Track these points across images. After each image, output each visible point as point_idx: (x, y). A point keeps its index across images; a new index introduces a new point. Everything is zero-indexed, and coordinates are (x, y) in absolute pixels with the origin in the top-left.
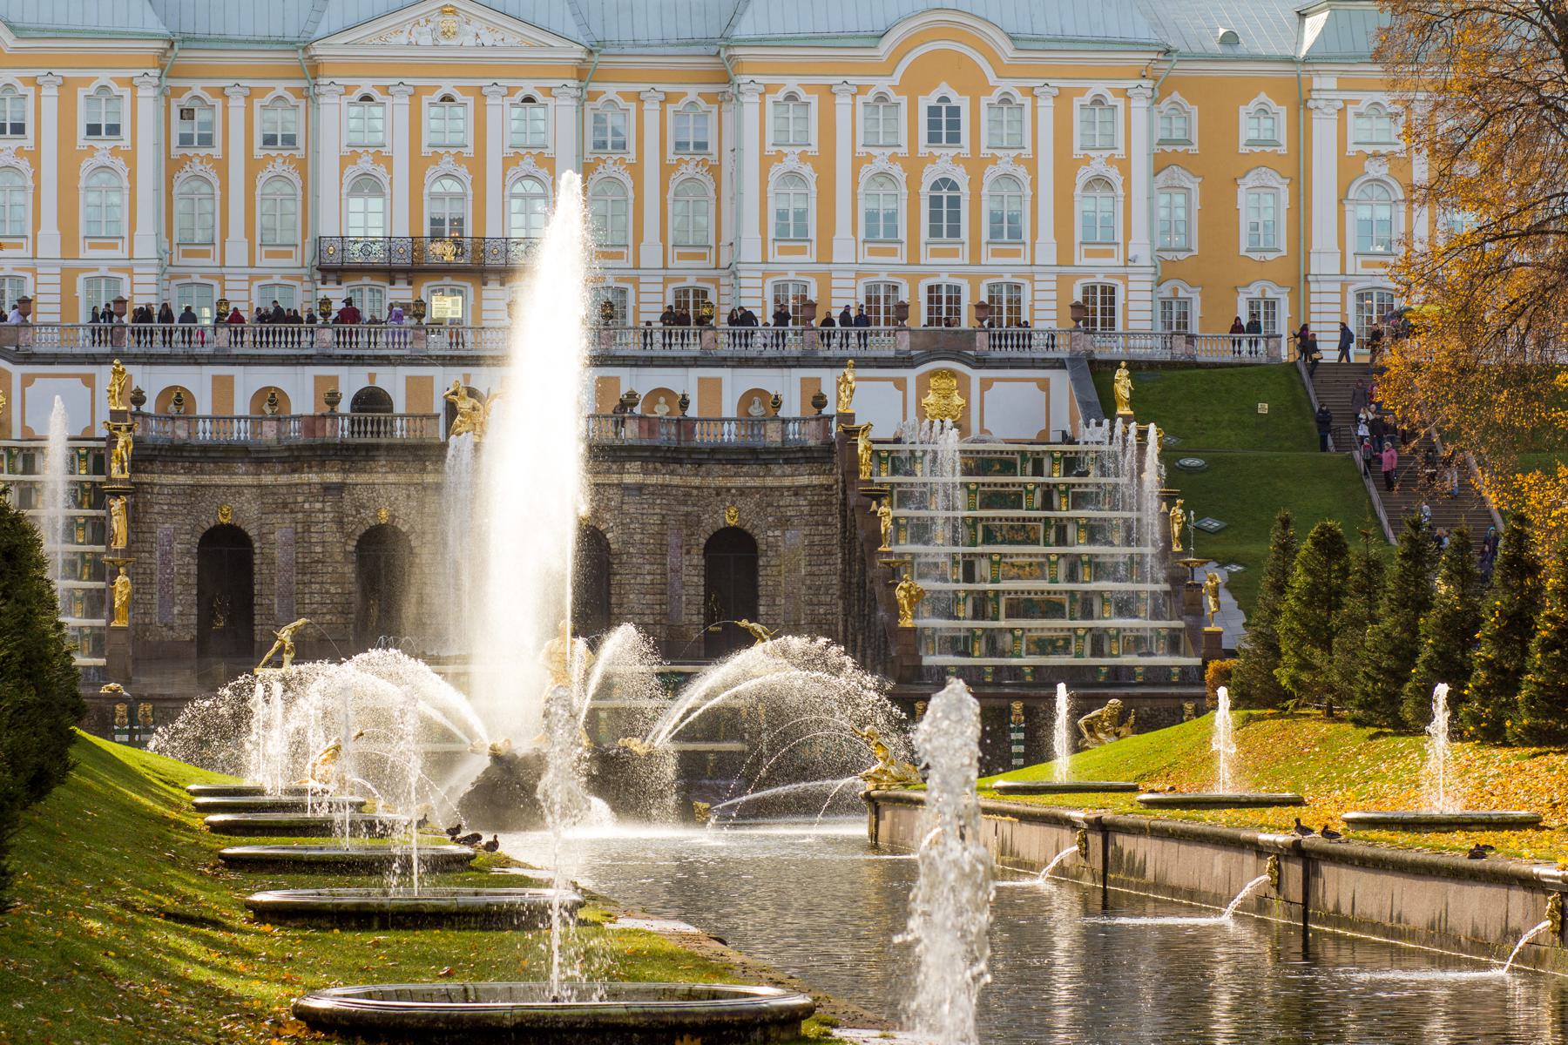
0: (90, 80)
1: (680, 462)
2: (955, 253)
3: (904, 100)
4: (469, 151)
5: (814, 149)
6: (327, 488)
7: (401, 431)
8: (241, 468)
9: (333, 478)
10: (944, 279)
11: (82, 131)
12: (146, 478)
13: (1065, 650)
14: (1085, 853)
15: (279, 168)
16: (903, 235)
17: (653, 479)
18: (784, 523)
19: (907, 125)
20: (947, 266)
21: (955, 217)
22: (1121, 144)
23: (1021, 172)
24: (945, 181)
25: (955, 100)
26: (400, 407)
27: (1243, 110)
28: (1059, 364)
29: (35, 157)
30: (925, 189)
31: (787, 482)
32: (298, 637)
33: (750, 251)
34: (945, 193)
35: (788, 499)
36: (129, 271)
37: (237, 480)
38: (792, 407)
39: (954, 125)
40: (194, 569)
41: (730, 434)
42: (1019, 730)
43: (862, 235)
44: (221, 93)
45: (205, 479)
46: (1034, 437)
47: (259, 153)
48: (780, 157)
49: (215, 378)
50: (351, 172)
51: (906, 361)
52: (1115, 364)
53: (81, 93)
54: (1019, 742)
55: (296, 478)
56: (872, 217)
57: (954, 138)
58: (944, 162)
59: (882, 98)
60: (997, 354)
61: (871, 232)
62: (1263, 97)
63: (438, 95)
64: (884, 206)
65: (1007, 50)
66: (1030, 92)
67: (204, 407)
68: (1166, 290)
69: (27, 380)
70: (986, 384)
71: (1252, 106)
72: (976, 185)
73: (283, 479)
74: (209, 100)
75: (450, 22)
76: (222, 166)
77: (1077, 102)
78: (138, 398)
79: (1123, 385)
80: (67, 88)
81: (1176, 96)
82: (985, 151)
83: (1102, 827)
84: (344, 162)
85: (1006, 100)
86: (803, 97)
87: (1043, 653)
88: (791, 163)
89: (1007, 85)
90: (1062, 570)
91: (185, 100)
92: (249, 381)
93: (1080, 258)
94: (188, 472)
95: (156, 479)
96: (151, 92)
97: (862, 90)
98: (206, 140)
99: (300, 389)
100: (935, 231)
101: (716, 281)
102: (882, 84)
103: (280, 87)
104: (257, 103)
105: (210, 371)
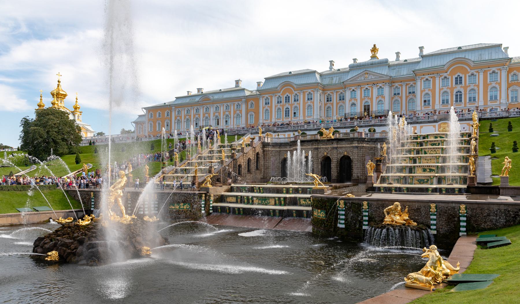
1: (369, 142)
3: (450, 77)
4: (370, 97)
11: (306, 99)
12: (266, 149)
13: (427, 182)
15: (341, 104)
17: (360, 145)
21: (461, 98)
22: (499, 79)
23: (476, 88)
24: (459, 91)
29: (299, 104)
30: (454, 93)
34: (459, 94)
39: (461, 81)
40: (280, 166)
42: (365, 211)
43: (441, 103)
45: (281, 149)
48: (424, 90)
50: (351, 103)
54: (365, 216)
56: (443, 100)
57: (461, 83)
58: (459, 88)
59: (445, 77)
61: (443, 103)
63: (365, 88)
64: (445, 98)
72: (465, 91)
75: (367, 76)
76: (332, 104)
77: (488, 73)
81: (515, 71)
82: (467, 84)
84: (350, 101)
85: (472, 74)
86: (429, 79)
87: (420, 183)
88: (427, 91)
89: (472, 71)
91: (327, 94)
93: (489, 103)
98: (331, 101)
102: (445, 74)
103: (341, 91)
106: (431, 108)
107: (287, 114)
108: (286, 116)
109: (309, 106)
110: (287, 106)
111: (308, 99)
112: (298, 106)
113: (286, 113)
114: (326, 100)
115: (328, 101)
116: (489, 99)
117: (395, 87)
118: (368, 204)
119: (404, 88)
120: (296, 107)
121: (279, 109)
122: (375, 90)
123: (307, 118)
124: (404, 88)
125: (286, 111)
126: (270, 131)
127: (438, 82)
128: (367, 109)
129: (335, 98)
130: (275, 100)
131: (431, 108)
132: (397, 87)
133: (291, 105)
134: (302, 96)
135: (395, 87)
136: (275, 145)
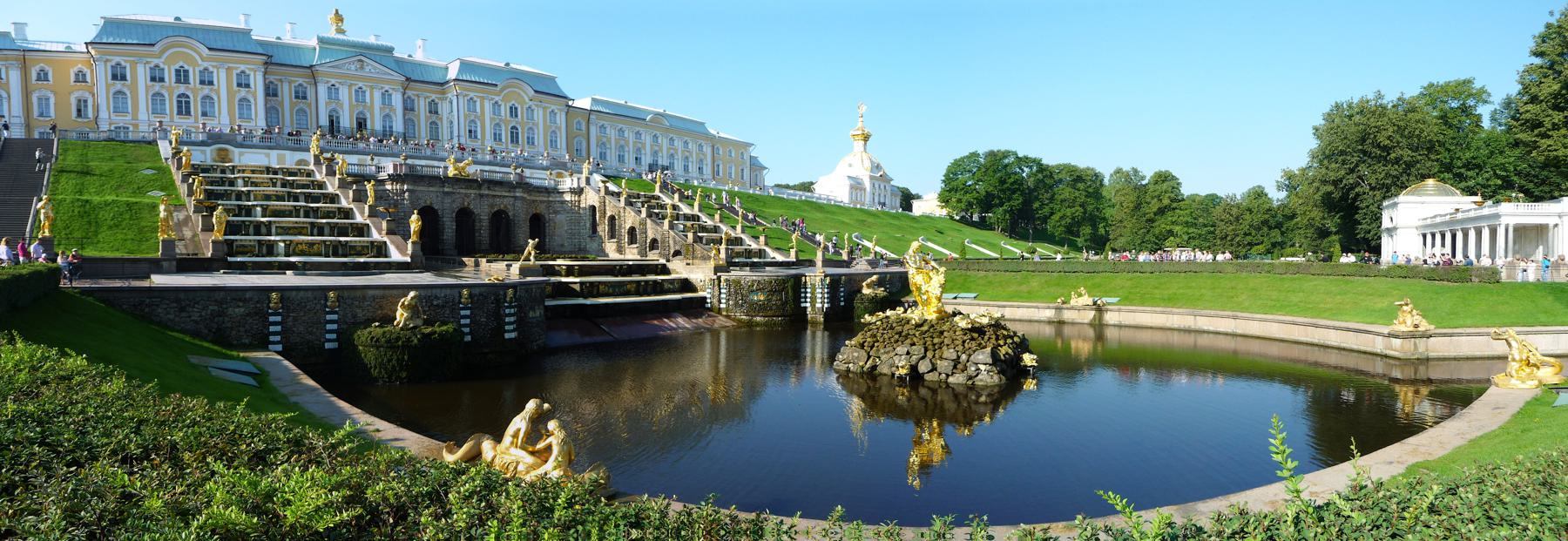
18: (556, 212)
76: (282, 103)
98: (275, 95)
103: (301, 81)
107: (184, 108)
108: (180, 113)
110: (182, 89)
111: (239, 85)
113: (179, 107)
119: (422, 102)
122: (377, 95)
124: (422, 102)
125: (179, 102)
127: (488, 106)
128: (361, 125)
129: (286, 92)
133: (194, 91)
134: (223, 74)
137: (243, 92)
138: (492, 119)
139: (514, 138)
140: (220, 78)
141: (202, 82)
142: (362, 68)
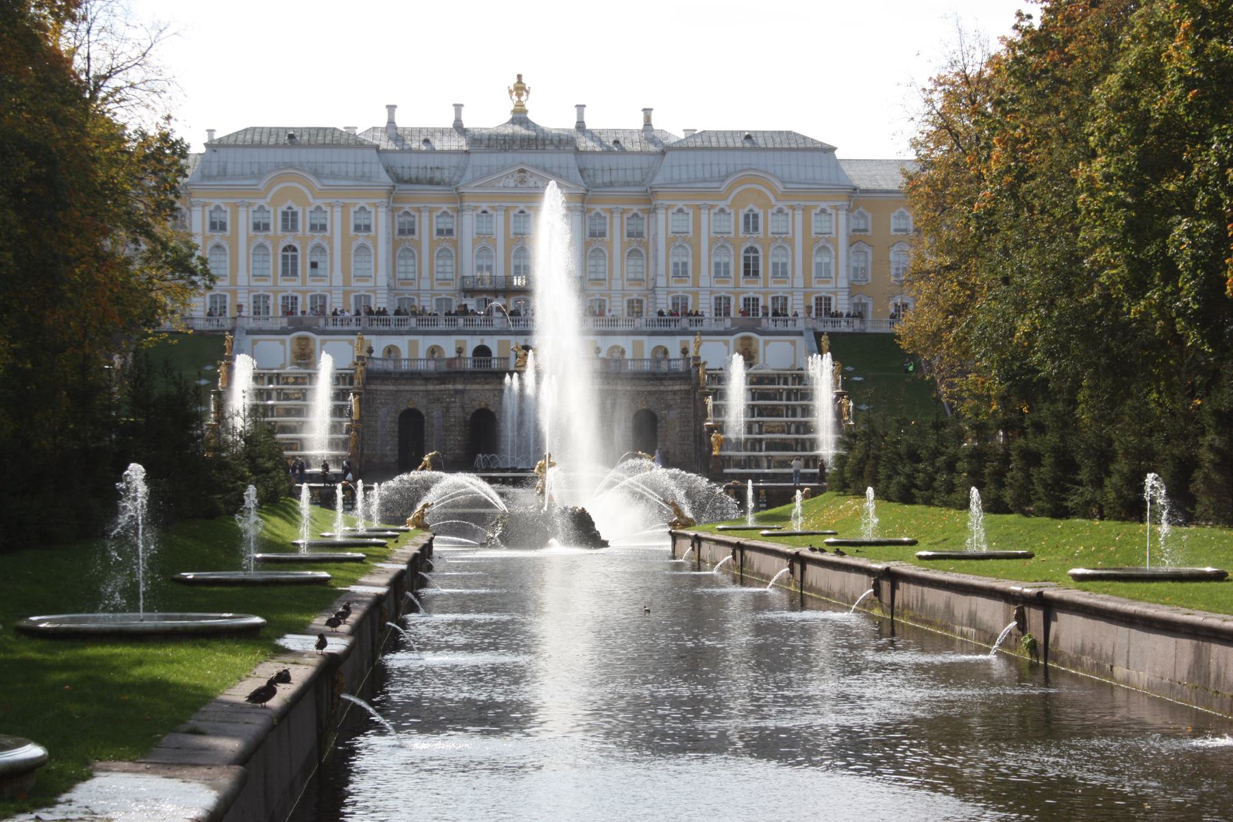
0: (355, 204)
2: (756, 282)
5: (691, 234)
6: (456, 391)
7: (495, 365)
8: (418, 382)
9: (460, 387)
10: (751, 295)
11: (352, 228)
12: (373, 387)
14: (734, 558)
15: (445, 245)
16: (732, 274)
18: (669, 407)
19: (732, 225)
20: (752, 288)
21: (756, 265)
25: (756, 210)
26: (495, 354)
27: (892, 216)
28: (800, 334)
29: (331, 239)
31: (670, 388)
32: (432, 459)
33: (661, 282)
34: (752, 255)
35: (670, 397)
36: (375, 292)
37: (416, 388)
38: (675, 353)
41: (647, 366)
43: (713, 274)
44: (419, 210)
45: (402, 388)
46: (788, 367)
47: (435, 237)
49: (410, 342)
51: (731, 333)
52: (822, 333)
53: (352, 210)
55: (442, 387)
56: (718, 265)
57: (756, 229)
59: (722, 211)
60: (421, 328)
61: (717, 273)
62: (902, 209)
65: (780, 187)
66: (793, 208)
67: (405, 354)
68: (856, 300)
69: (323, 342)
70: (766, 343)
71: (896, 213)
73: (438, 387)
74: (413, 213)
76: (418, 244)
77: (813, 212)
78: (370, 351)
79: (825, 340)
80: (344, 206)
81: (861, 209)
83: (739, 547)
84: (474, 242)
85: (780, 211)
86: (686, 210)
87: (781, 467)
89: (780, 205)
90: (793, 429)
91: (401, 213)
92: (425, 343)
93: (814, 284)
94: (394, 384)
95: (378, 387)
96: (384, 209)
97: (712, 207)
98: (412, 232)
99: (448, 346)
100: (747, 273)
101: (646, 296)
102: (722, 204)
103: (445, 207)
104: (435, 215)
105: (407, 338)
106: (690, 282)
108: (285, 273)
109: (363, 247)
110: (289, 239)
111: (357, 228)
112: (325, 245)
113: (285, 264)
114: (397, 232)
115: (401, 232)
116: (814, 275)
117: (593, 214)
118: (766, 494)
119: (617, 220)
120: (319, 249)
121: (261, 246)
123: (355, 284)
124: (617, 220)
125: (285, 258)
126: (309, 329)
130: (244, 221)
131: (690, 282)
132: (598, 214)
135: (593, 214)
136: (385, 376)
137: (362, 237)
138: (712, 242)
139: (751, 269)
140: (335, 220)
141: (313, 227)
142: (522, 181)
